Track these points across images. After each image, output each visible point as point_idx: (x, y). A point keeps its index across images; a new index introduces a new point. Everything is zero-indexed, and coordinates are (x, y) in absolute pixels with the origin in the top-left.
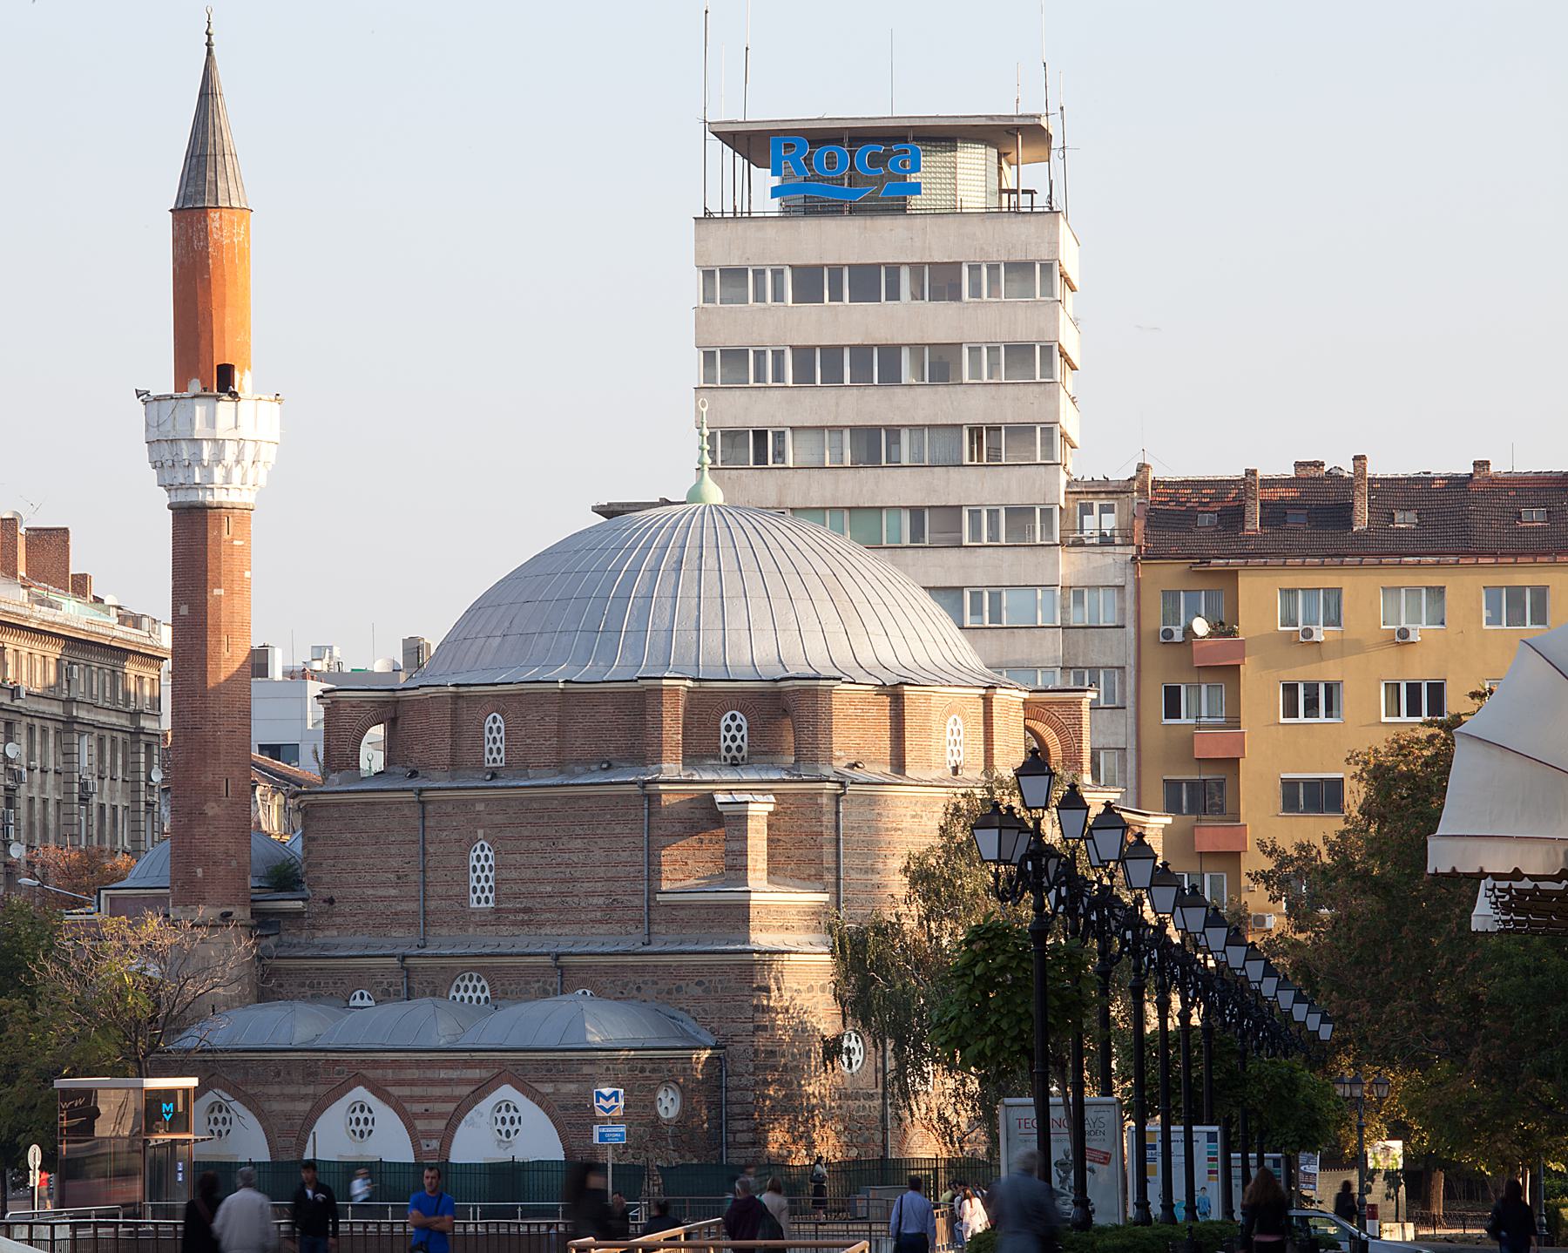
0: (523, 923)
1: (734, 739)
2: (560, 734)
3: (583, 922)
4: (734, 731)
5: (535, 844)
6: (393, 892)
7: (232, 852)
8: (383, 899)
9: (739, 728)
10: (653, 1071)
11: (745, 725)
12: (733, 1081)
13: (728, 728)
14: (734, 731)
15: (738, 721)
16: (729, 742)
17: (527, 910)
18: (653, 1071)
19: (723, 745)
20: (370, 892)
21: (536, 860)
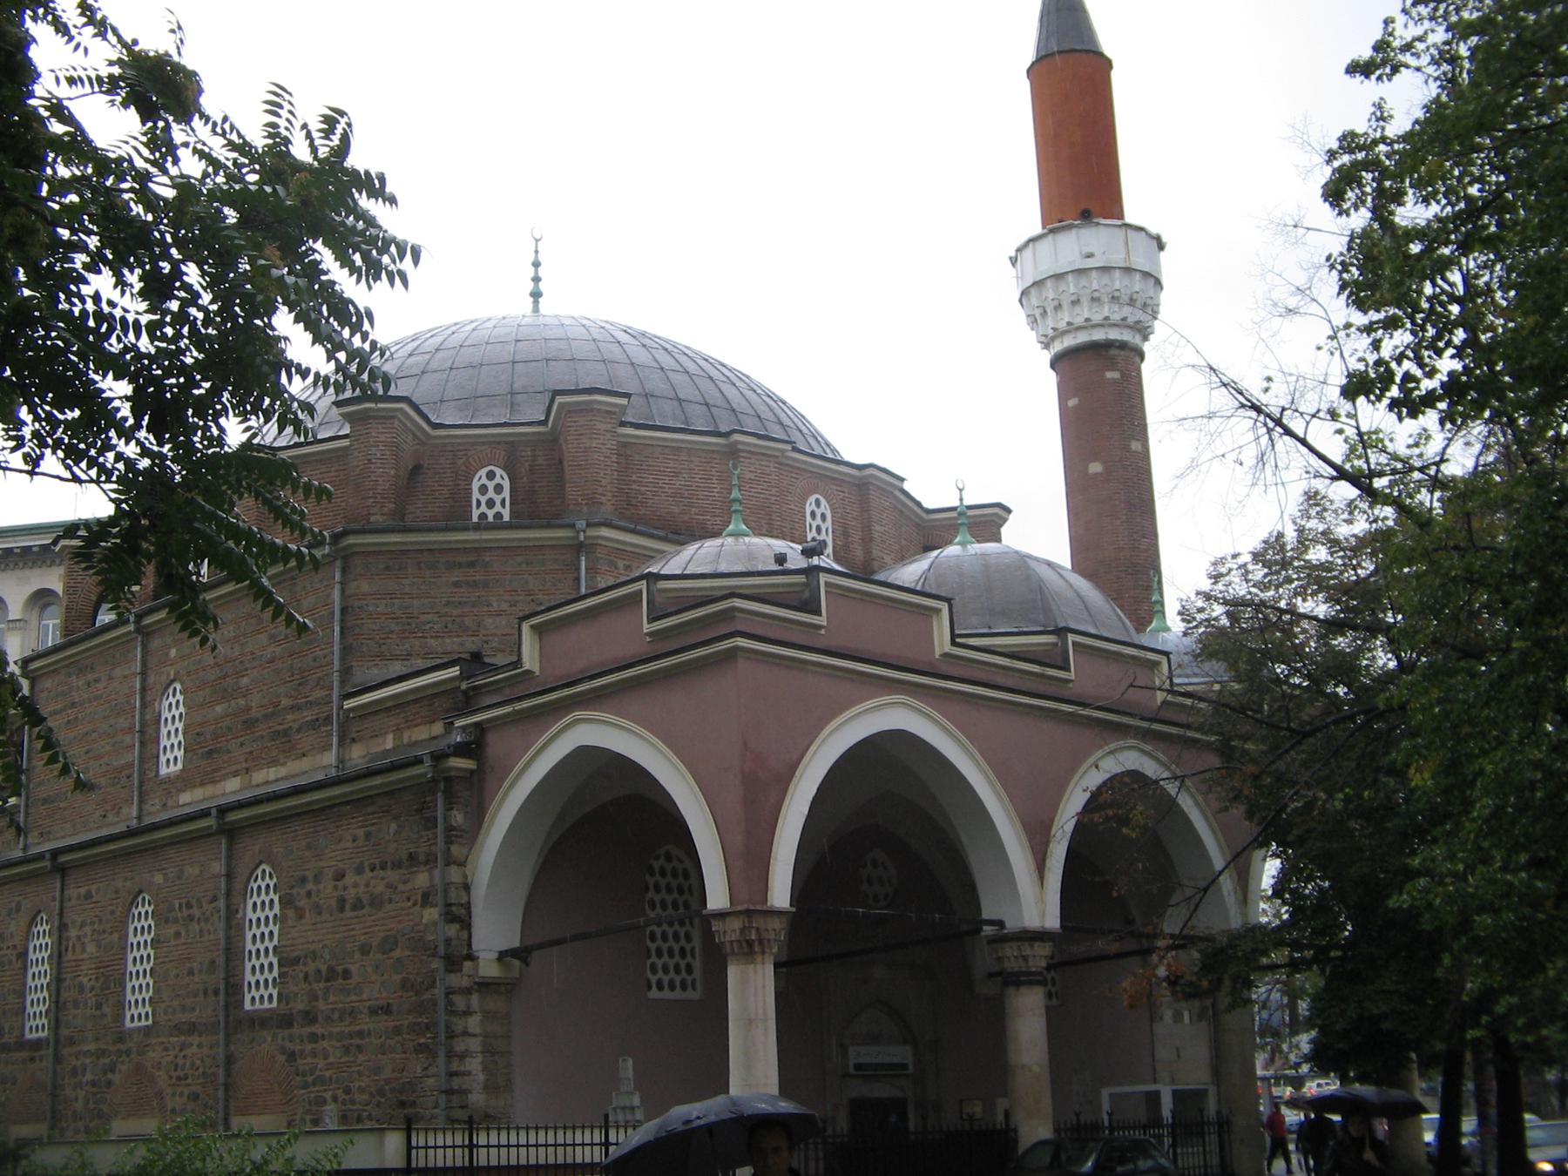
1: (490, 504)
4: (491, 494)
9: (498, 489)
11: (506, 484)
13: (483, 489)
14: (491, 494)
15: (498, 480)
16: (484, 508)
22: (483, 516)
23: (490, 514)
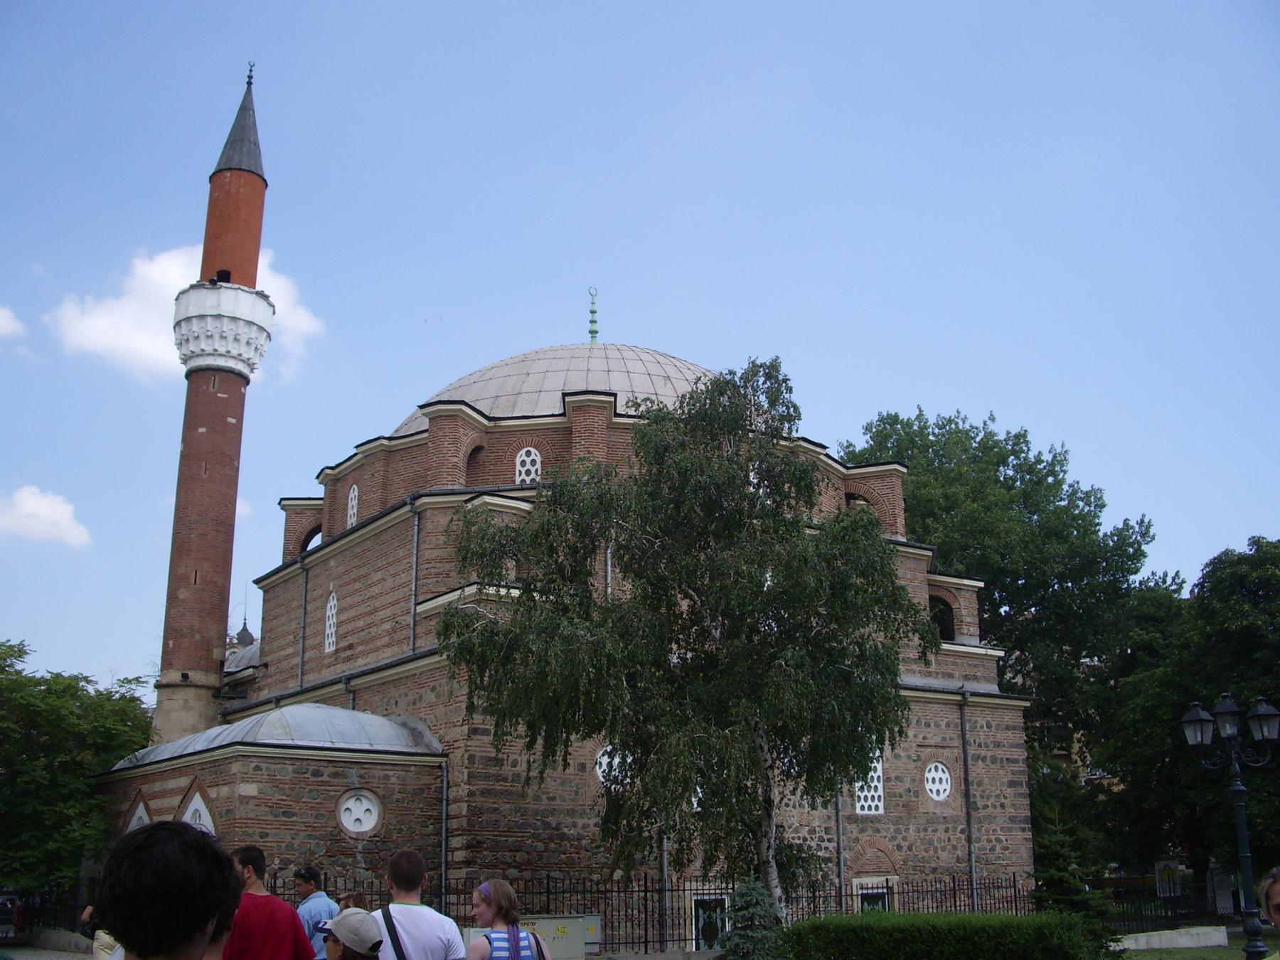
0: (349, 659)
1: (528, 473)
2: (384, 486)
3: (377, 649)
4: (528, 466)
5: (357, 585)
6: (291, 650)
7: (196, 628)
8: (287, 657)
9: (533, 462)
10: (336, 775)
11: (539, 460)
12: (453, 793)
13: (523, 463)
14: (528, 466)
16: (523, 476)
17: (350, 647)
18: (336, 775)
19: (518, 480)
20: (283, 653)
21: (357, 598)
22: (523, 481)
23: (528, 480)
